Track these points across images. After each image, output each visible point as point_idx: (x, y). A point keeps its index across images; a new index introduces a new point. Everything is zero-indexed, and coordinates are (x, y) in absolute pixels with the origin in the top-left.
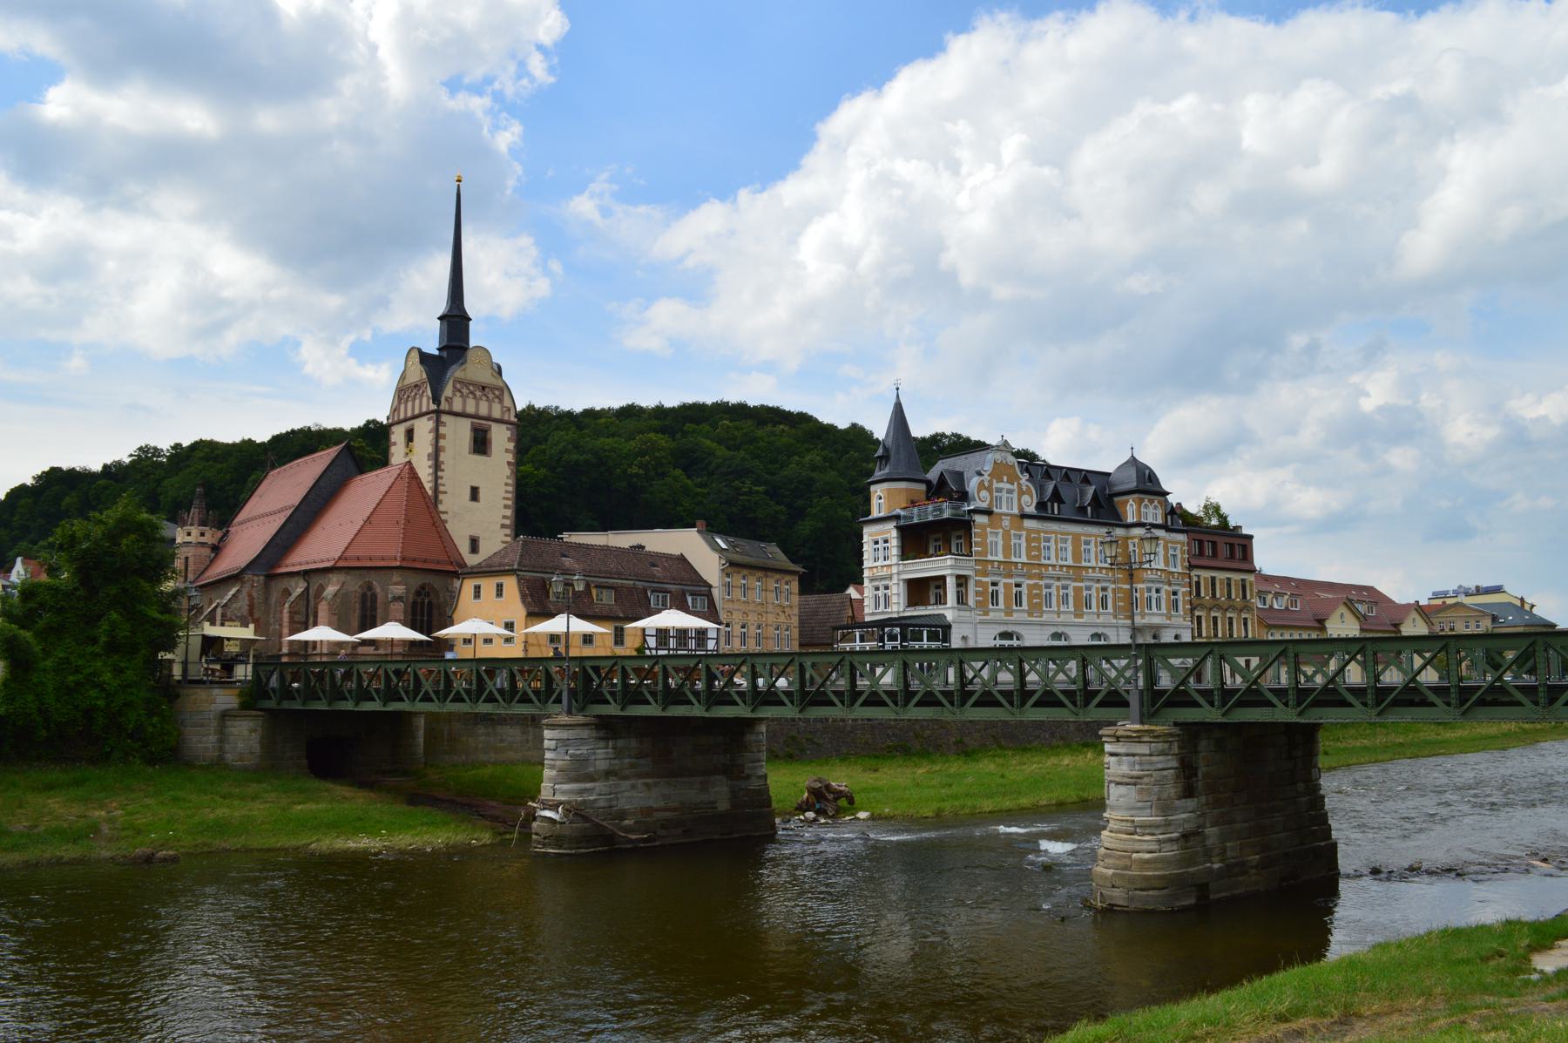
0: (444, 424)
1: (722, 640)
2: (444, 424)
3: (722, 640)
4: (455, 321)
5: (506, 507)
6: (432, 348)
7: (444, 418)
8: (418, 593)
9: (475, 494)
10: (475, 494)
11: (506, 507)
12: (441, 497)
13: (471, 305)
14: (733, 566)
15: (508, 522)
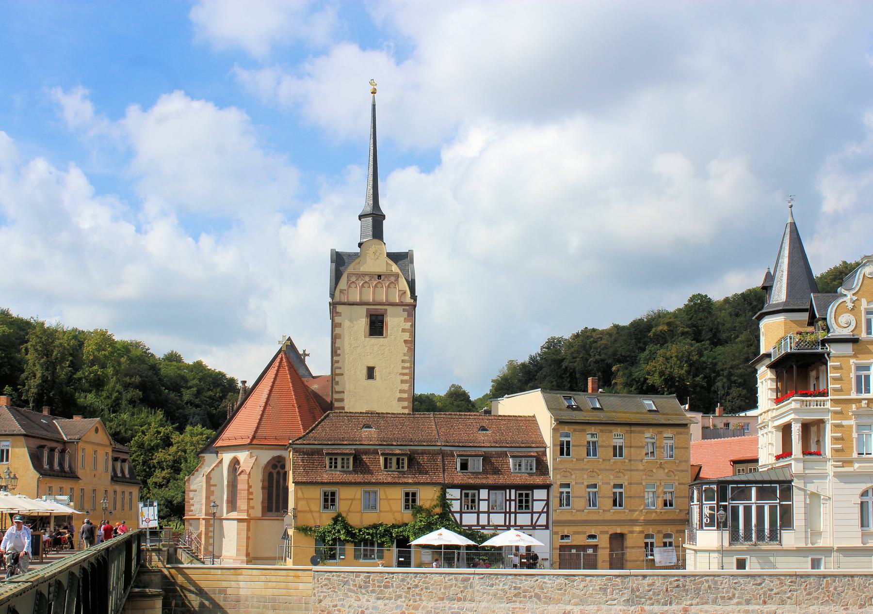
0: (339, 314)
1: (554, 502)
2: (339, 314)
3: (554, 502)
4: (376, 219)
5: (402, 382)
6: (349, 246)
7: (340, 308)
8: (274, 466)
9: (371, 373)
10: (371, 373)
11: (402, 382)
12: (337, 378)
13: (384, 205)
14: (561, 423)
15: (405, 395)
